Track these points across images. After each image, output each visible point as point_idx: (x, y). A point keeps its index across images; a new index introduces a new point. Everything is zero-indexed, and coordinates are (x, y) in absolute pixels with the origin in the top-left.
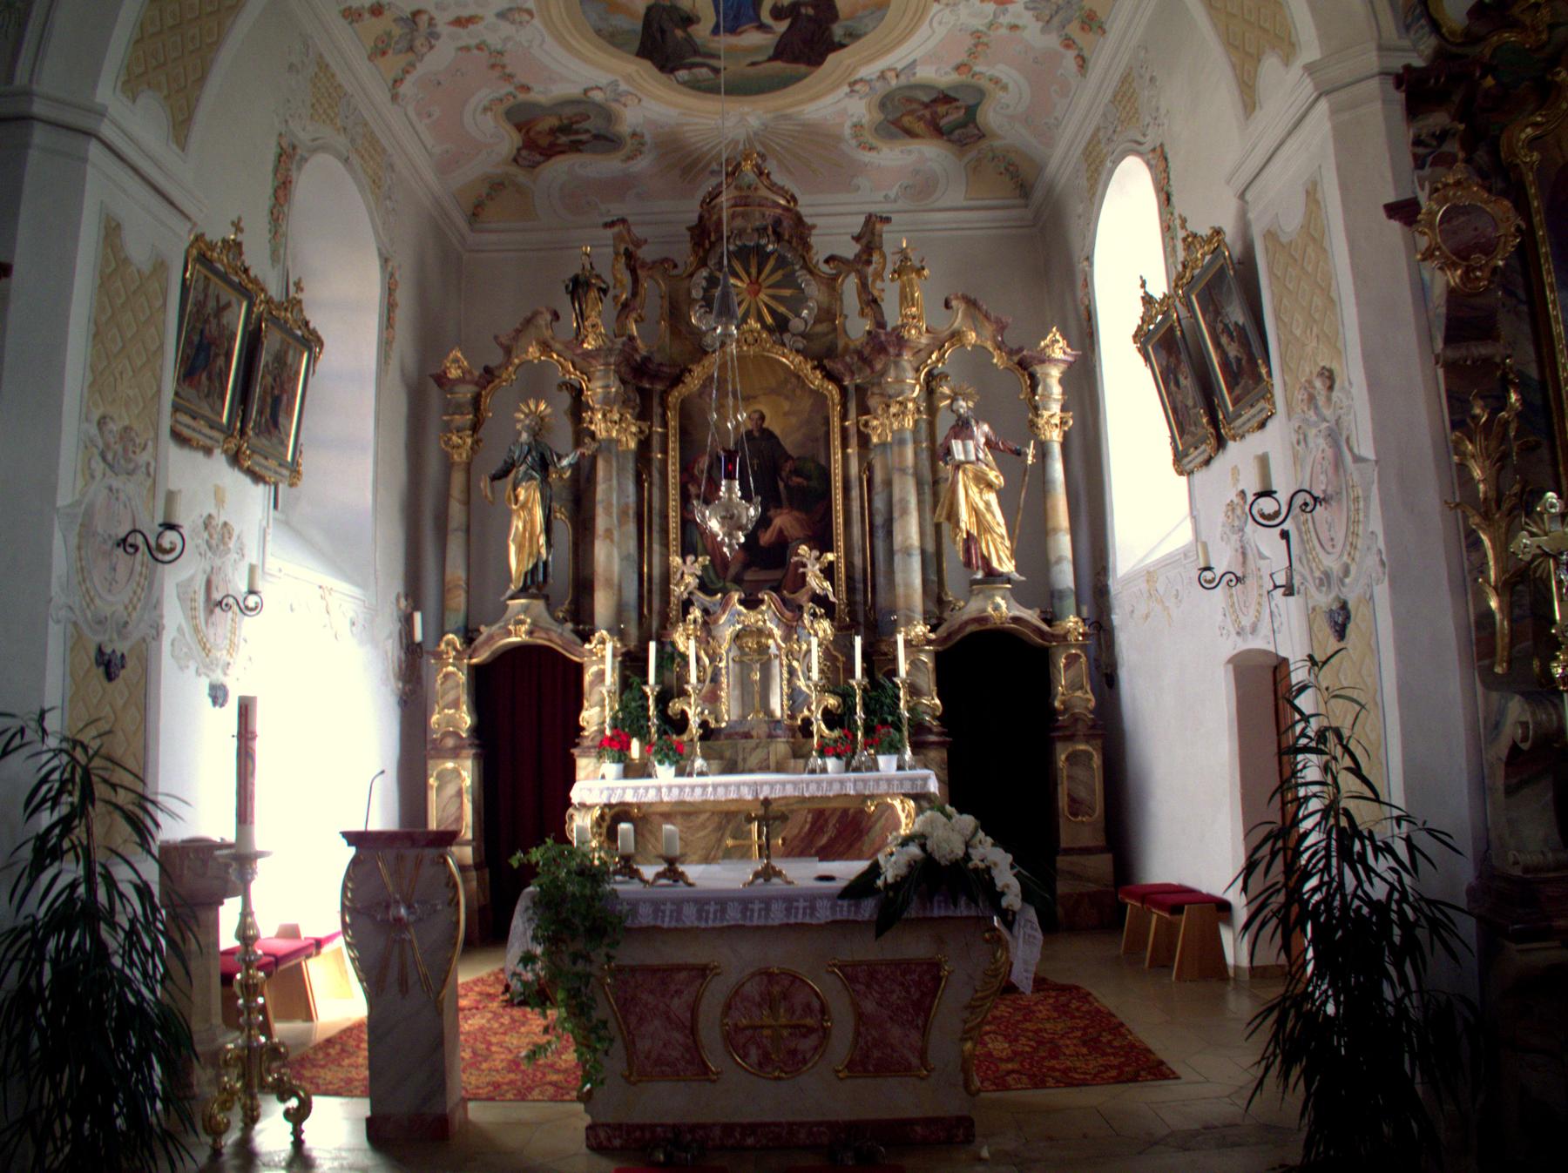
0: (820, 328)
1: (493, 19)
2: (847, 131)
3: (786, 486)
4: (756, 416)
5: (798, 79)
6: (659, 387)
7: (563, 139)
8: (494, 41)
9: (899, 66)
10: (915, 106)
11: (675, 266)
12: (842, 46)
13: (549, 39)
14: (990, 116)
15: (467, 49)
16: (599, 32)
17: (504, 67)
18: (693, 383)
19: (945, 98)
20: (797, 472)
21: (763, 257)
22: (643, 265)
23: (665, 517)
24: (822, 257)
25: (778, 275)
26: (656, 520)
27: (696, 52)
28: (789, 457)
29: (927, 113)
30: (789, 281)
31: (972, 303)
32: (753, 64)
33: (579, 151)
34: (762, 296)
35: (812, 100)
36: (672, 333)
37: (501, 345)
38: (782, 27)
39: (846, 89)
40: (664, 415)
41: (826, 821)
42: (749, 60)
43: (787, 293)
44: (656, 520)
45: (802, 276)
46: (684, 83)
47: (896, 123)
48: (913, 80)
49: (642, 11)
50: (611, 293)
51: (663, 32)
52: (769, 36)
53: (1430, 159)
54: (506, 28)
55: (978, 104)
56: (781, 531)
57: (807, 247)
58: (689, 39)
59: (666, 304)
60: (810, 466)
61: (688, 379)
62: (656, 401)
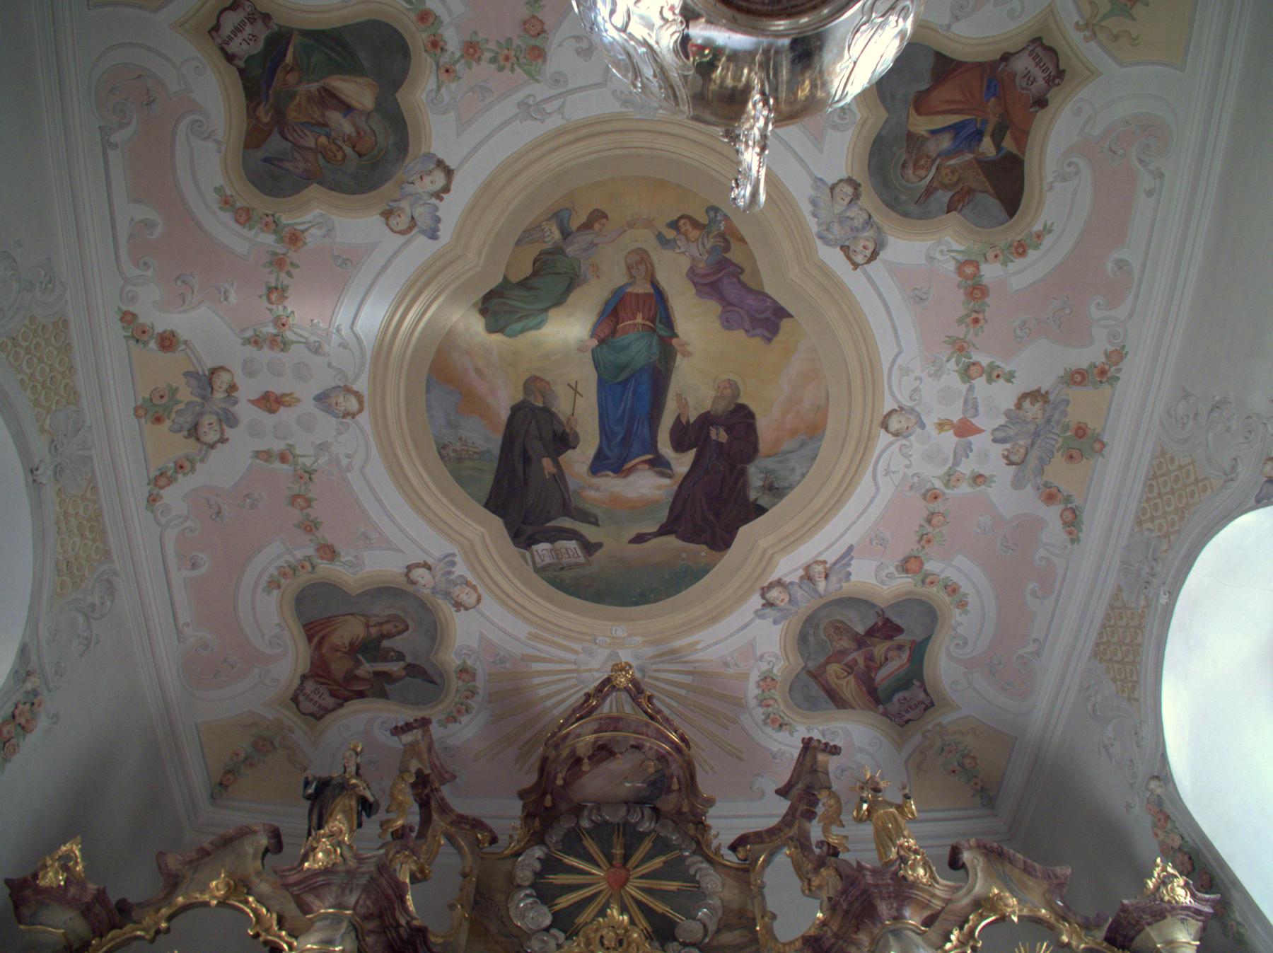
0: (728, 938)
1: (308, 405)
2: (753, 690)
7: (367, 668)
8: (304, 446)
9: (831, 557)
10: (845, 643)
11: (494, 840)
12: (761, 511)
13: (375, 454)
14: (944, 666)
15: (266, 455)
16: (442, 448)
17: (309, 502)
19: (886, 628)
21: (632, 838)
22: (444, 809)
24: (728, 838)
25: (657, 862)
27: (567, 509)
29: (858, 657)
30: (674, 870)
31: (994, 855)
32: (640, 539)
33: (384, 695)
34: (630, 889)
35: (715, 618)
36: (472, 931)
37: (162, 868)
38: (682, 463)
39: (756, 601)
43: (672, 886)
45: (697, 865)
46: (541, 571)
47: (817, 675)
48: (847, 588)
49: (504, 415)
50: (381, 815)
51: (527, 460)
52: (667, 481)
54: (326, 425)
55: (929, 638)
57: (702, 826)
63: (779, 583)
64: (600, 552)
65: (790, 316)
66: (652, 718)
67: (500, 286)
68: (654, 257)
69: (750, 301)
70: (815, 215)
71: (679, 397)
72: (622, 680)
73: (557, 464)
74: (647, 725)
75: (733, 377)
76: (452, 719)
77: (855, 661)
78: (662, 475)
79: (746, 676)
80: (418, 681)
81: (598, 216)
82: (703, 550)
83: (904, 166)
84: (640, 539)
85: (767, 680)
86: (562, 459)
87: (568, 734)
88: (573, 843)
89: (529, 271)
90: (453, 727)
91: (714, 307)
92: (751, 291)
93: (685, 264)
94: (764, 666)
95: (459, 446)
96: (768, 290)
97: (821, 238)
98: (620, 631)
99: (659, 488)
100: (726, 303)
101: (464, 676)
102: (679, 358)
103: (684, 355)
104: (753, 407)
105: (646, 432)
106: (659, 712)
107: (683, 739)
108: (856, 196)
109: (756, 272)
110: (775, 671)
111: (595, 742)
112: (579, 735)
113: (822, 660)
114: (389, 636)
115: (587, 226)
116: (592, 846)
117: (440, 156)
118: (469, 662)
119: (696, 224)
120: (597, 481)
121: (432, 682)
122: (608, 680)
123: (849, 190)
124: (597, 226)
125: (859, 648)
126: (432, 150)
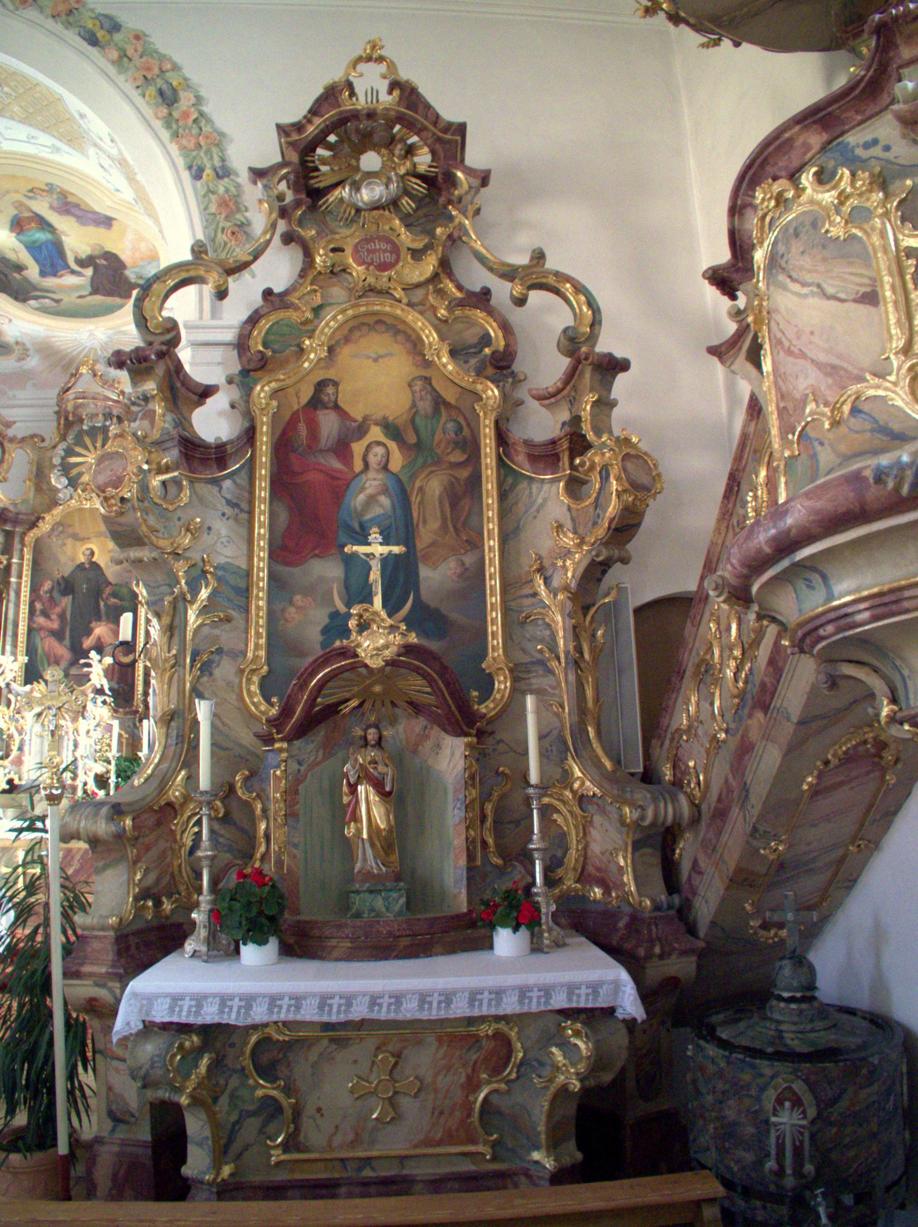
3: (106, 604)
4: (88, 552)
6: (19, 529)
11: (43, 440)
18: (44, 527)
20: (115, 595)
23: (16, 625)
26: (10, 627)
28: (110, 583)
32: (81, 297)
38: (89, 272)
40: (22, 550)
41: (73, 858)
42: (77, 295)
44: (10, 627)
53: (140, 415)
56: (99, 638)
58: (26, 280)
59: (35, 468)
60: (124, 590)
61: (41, 524)
62: (17, 539)
69: (90, 215)
71: (72, 251)
84: (81, 297)
88: (79, 441)
98: (91, 327)
100: (78, 218)
104: (114, 251)
116: (87, 440)
119: (43, 191)
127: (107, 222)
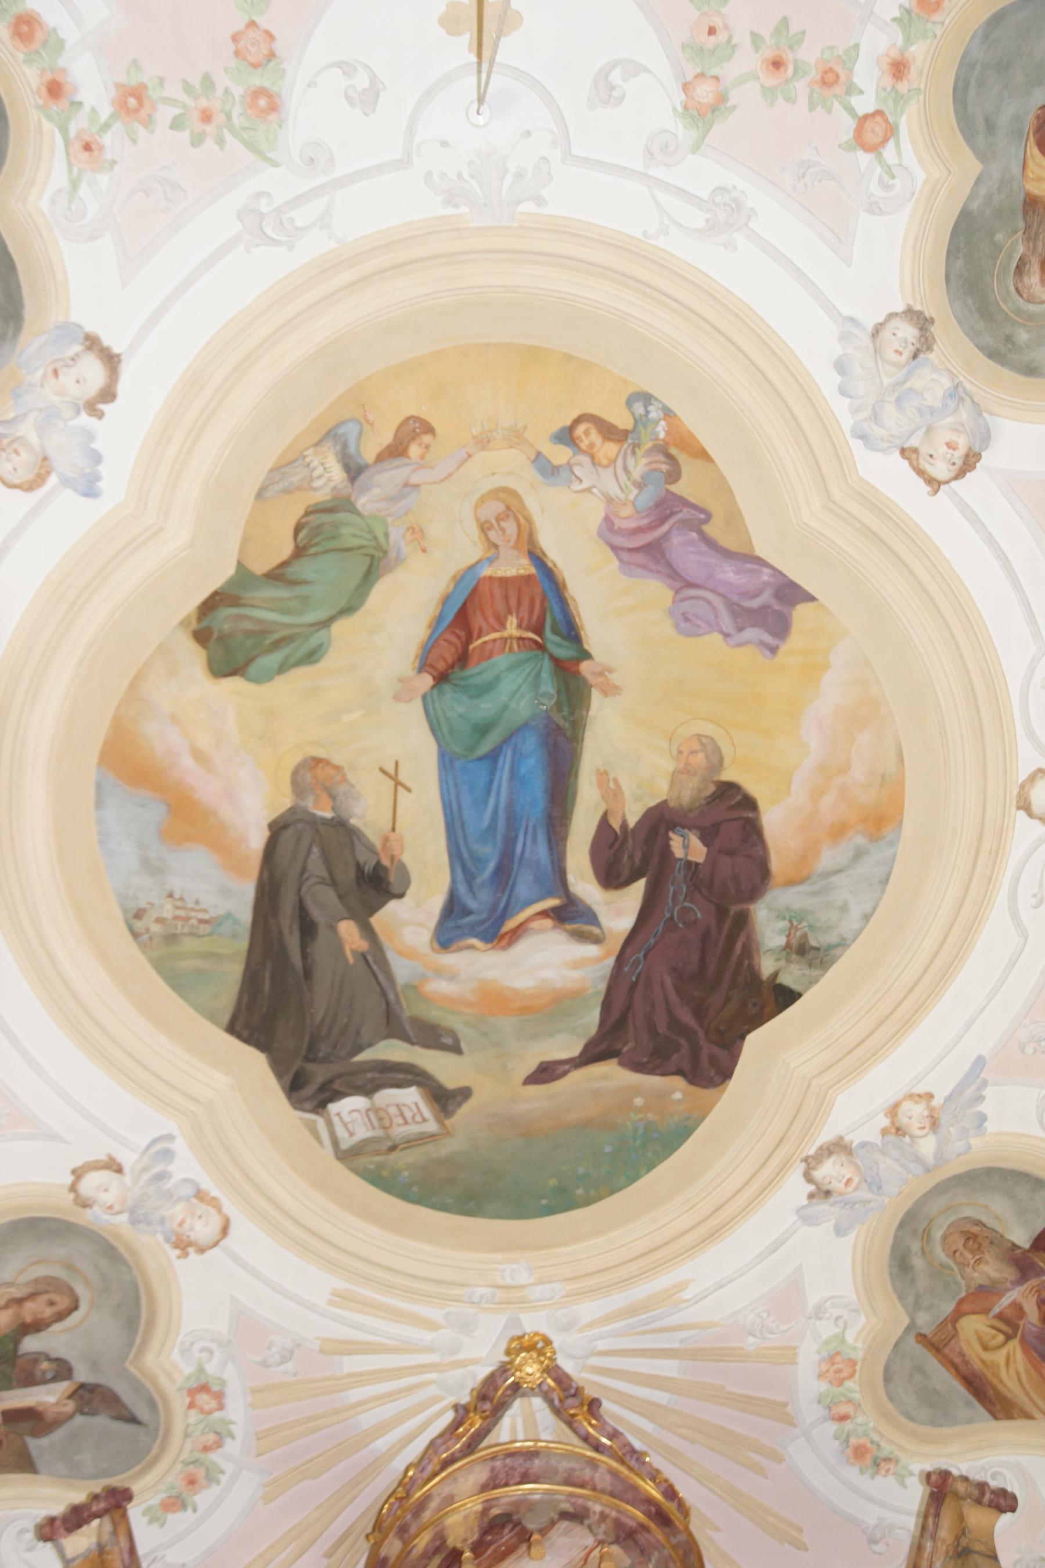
2: (807, 1384)
5: (664, 1140)
12: (786, 997)
27: (393, 1025)
32: (546, 1073)
35: (712, 1231)
39: (795, 1188)
46: (348, 1156)
47: (938, 1343)
48: (979, 1149)
49: (257, 840)
51: (308, 929)
52: (591, 950)
63: (838, 1147)
64: (466, 1108)
65: (812, 599)
66: (598, 1447)
67: (232, 582)
68: (532, 504)
69: (729, 574)
70: (843, 391)
71: (603, 776)
72: (531, 1370)
73: (369, 932)
74: (592, 1463)
75: (709, 729)
76: (175, 1503)
77: (1018, 1308)
78: (582, 937)
79: (788, 1355)
80: (101, 1421)
81: (414, 431)
82: (676, 1088)
83: (1020, 269)
85: (837, 1366)
86: (377, 920)
87: (427, 1498)
89: (287, 549)
90: (177, 1520)
91: (656, 591)
92: (727, 554)
93: (594, 512)
94: (827, 1329)
95: (168, 911)
96: (760, 551)
97: (863, 437)
99: (576, 965)
100: (681, 583)
101: (203, 1399)
102: (596, 695)
103: (605, 693)
104: (752, 786)
105: (542, 851)
106: (614, 1435)
107: (671, 1493)
108: (925, 343)
109: (734, 517)
110: (849, 1338)
111: (485, 1511)
112: (450, 1499)
113: (947, 1308)
114: (37, 1326)
115: (396, 451)
117: (90, 328)
118: (211, 1368)
120: (449, 959)
121: (133, 1420)
122: (504, 1369)
123: (908, 332)
124: (414, 450)
125: (1023, 1278)
126: (74, 318)
127: (772, 608)
